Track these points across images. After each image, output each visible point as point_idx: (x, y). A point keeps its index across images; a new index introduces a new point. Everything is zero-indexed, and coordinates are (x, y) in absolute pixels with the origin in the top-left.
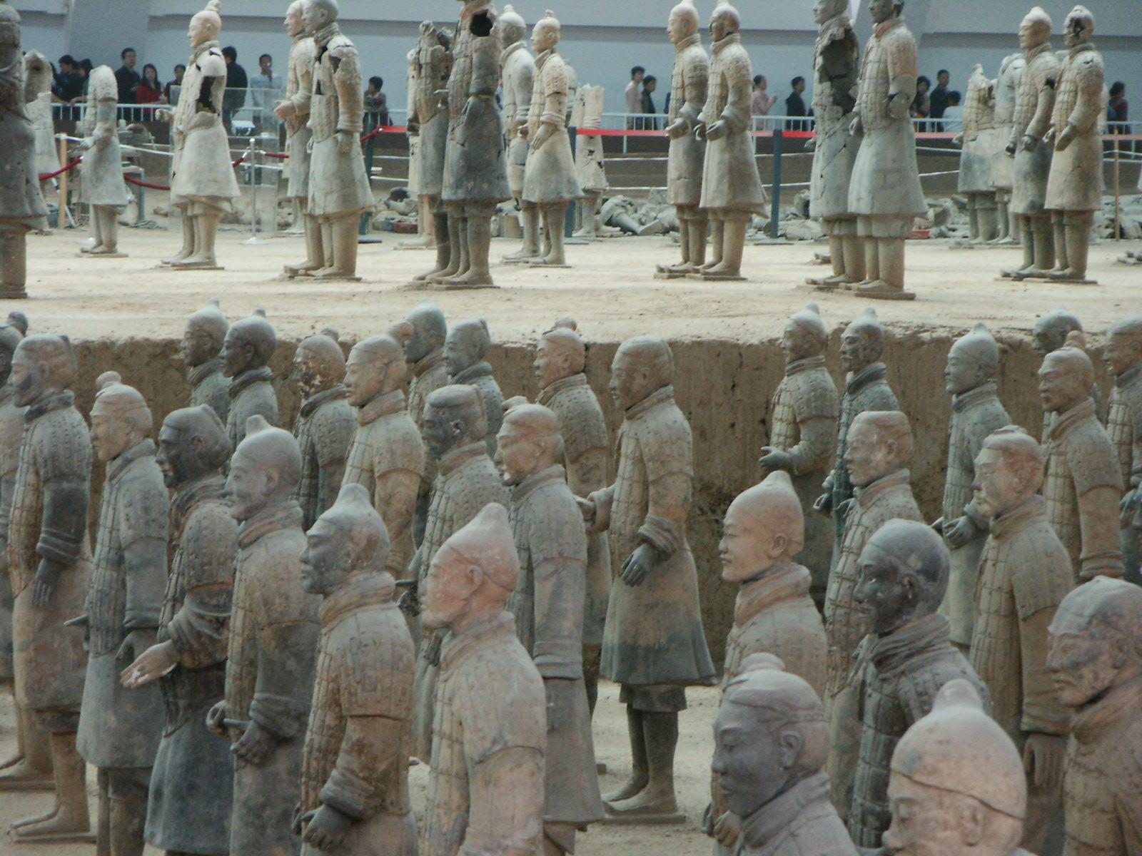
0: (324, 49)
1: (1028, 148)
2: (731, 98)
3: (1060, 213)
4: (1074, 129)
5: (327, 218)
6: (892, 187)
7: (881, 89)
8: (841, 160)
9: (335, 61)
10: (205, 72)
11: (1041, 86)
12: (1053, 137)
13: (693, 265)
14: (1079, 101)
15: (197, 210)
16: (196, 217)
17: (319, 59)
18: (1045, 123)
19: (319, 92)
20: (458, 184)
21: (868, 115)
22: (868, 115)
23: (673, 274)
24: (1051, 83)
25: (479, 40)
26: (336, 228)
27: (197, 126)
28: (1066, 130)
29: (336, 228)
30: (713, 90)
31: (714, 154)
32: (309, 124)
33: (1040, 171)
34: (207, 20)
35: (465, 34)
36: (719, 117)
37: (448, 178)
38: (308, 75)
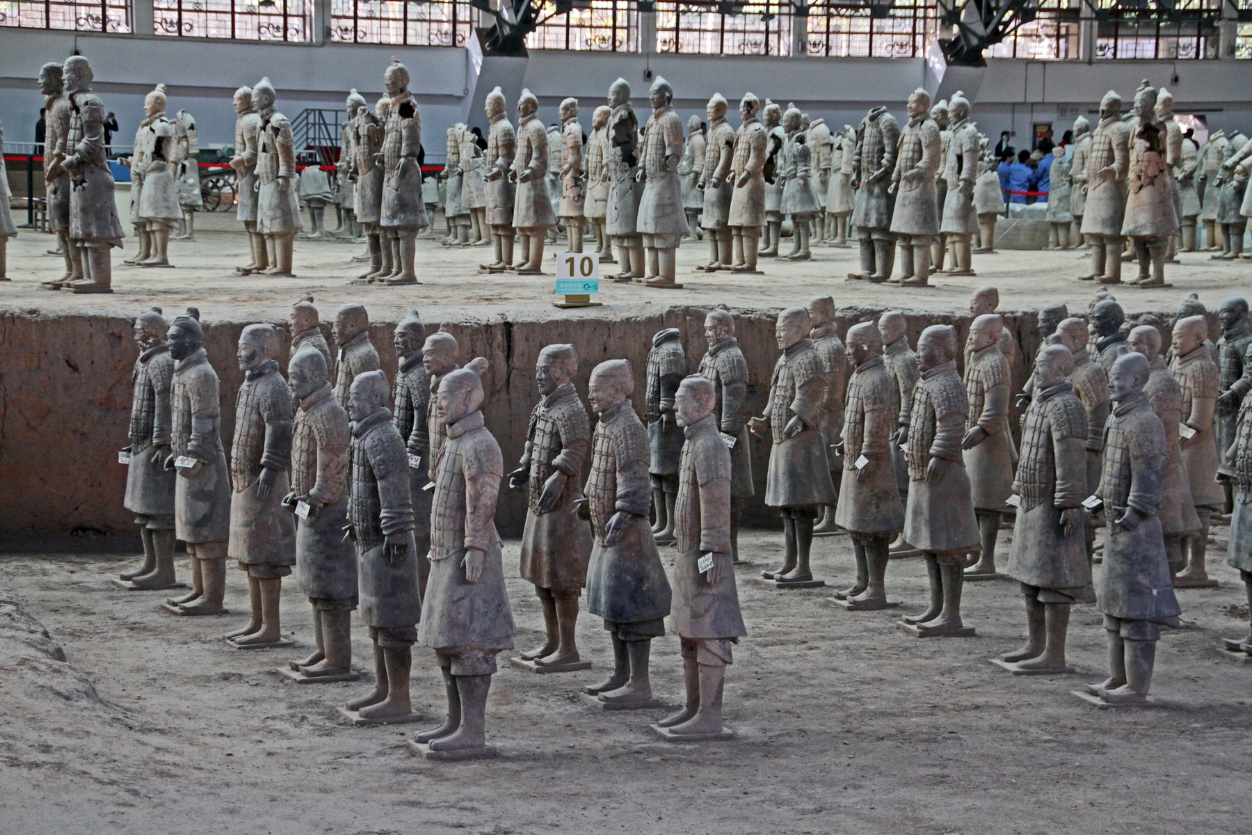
0: (267, 122)
1: (715, 186)
2: (534, 155)
3: (739, 228)
4: (749, 173)
5: (272, 236)
6: (668, 215)
7: (660, 152)
8: (629, 198)
9: (276, 130)
10: (158, 133)
11: (722, 144)
12: (734, 178)
13: (504, 264)
14: (752, 154)
15: (155, 227)
16: (153, 232)
17: (264, 128)
18: (727, 169)
19: (264, 150)
20: (393, 216)
21: (650, 169)
22: (650, 169)
23: (493, 271)
24: (730, 144)
25: (406, 122)
26: (278, 242)
27: (153, 170)
28: (744, 175)
29: (278, 242)
30: (520, 151)
31: (522, 193)
32: (256, 172)
33: (725, 201)
34: (158, 98)
35: (395, 116)
36: (526, 167)
37: (385, 212)
38: (254, 140)
